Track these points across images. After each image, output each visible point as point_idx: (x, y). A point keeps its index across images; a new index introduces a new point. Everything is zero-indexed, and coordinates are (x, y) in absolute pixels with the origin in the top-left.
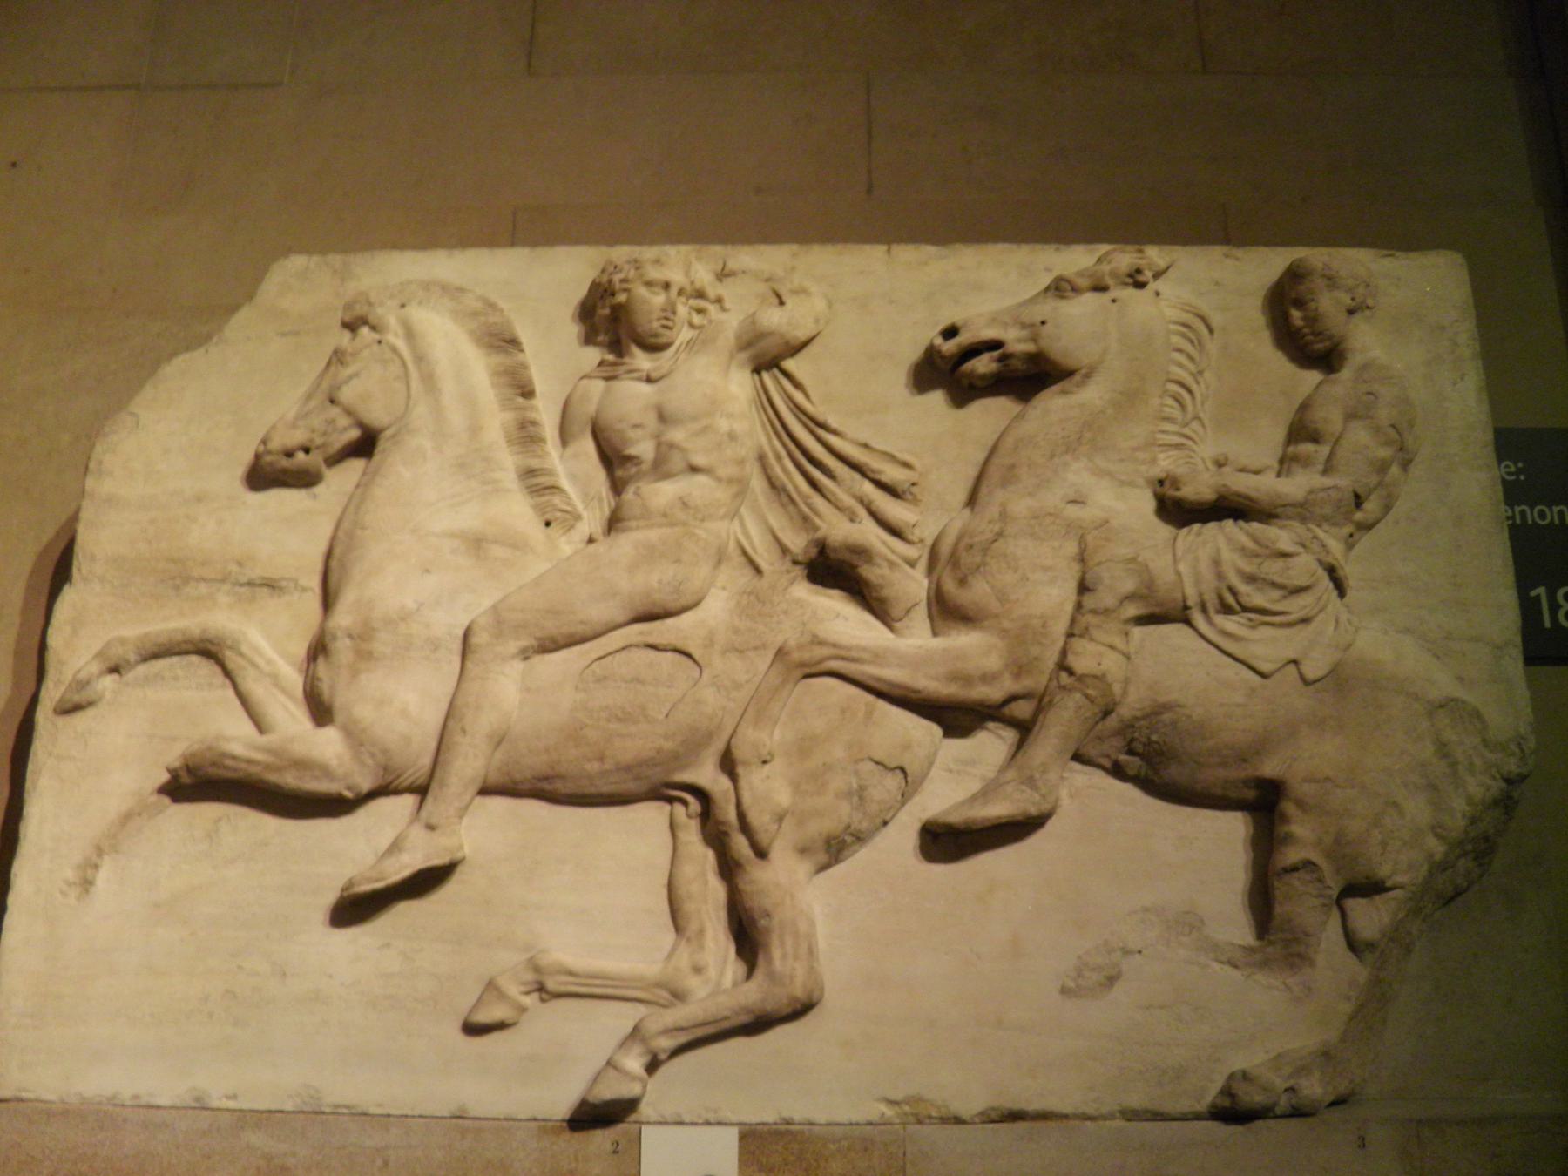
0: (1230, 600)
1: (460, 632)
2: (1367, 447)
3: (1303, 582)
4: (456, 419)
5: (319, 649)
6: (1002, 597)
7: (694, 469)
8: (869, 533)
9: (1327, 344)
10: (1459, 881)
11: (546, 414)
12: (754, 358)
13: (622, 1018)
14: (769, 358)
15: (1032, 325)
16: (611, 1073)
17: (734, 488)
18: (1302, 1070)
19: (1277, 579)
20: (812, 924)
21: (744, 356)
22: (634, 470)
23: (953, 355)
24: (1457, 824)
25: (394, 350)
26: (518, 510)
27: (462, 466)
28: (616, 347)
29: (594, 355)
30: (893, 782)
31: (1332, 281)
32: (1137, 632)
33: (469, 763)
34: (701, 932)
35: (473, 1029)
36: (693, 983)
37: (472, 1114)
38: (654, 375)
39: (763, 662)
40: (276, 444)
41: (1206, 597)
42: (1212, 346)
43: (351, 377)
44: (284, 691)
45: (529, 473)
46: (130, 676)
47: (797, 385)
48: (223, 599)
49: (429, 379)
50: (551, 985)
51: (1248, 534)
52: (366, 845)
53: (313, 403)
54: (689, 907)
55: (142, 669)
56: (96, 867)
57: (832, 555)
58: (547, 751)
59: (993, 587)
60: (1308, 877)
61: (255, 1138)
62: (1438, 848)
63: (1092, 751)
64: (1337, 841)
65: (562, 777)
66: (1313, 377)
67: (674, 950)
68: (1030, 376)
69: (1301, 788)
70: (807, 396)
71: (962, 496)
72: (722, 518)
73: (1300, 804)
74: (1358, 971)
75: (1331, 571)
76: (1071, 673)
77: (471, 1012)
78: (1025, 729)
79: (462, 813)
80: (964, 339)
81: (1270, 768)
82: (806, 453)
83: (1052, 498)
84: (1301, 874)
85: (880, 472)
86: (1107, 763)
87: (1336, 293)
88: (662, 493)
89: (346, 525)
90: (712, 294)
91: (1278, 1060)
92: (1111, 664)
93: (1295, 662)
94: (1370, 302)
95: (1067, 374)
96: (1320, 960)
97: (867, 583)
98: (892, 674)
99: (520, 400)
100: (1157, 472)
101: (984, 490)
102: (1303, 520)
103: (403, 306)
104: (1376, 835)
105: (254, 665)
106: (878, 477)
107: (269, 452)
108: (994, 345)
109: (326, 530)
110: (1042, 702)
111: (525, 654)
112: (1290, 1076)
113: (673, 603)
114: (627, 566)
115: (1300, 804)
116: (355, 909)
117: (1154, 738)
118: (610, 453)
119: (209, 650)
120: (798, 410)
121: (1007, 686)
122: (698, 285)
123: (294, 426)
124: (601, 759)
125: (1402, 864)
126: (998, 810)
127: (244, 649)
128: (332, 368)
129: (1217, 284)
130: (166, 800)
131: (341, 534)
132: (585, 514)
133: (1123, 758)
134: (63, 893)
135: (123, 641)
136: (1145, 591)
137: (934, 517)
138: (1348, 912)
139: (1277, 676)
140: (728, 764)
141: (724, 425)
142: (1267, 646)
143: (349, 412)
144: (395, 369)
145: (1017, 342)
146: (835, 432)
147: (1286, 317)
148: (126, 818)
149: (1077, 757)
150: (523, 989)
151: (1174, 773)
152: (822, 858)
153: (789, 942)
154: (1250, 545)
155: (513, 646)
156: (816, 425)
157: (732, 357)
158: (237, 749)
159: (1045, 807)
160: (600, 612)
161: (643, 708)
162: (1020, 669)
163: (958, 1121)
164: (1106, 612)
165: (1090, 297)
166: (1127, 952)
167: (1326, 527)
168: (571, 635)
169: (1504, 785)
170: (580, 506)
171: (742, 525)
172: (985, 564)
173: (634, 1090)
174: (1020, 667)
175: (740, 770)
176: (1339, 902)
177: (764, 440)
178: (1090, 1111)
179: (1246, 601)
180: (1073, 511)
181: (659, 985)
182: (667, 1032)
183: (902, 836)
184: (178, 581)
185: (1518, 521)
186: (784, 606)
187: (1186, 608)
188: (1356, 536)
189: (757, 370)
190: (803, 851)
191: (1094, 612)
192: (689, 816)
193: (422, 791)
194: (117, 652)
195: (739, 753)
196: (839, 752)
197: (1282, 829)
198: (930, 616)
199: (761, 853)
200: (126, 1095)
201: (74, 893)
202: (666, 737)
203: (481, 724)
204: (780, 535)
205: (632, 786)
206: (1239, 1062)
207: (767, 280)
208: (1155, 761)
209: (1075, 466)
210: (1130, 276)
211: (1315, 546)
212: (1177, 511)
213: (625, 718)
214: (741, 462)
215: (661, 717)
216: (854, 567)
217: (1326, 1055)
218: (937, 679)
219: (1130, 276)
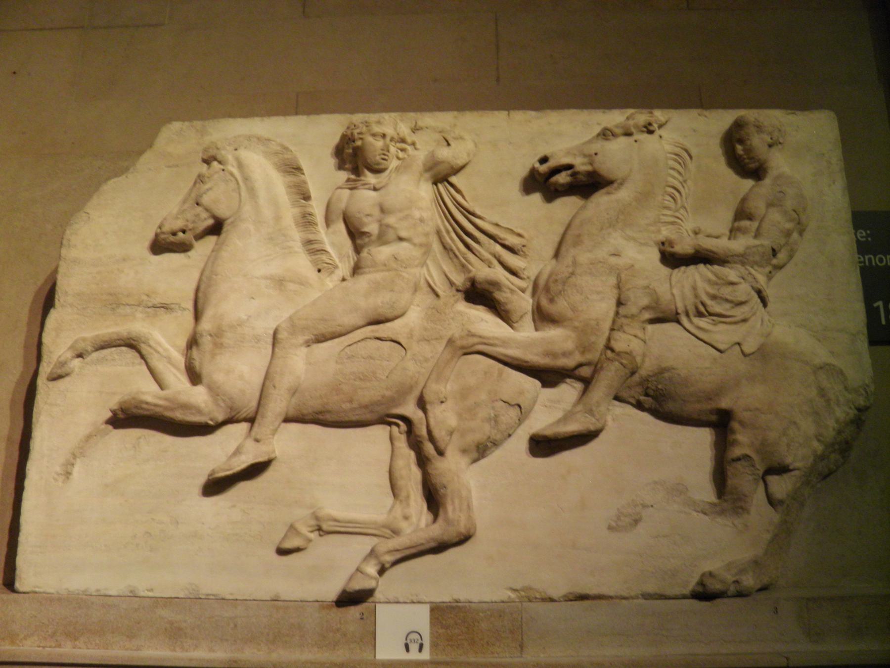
0: (702, 309)
1: (272, 332)
2: (779, 223)
3: (743, 299)
4: (267, 212)
5: (193, 342)
6: (574, 309)
7: (401, 239)
8: (500, 274)
9: (757, 164)
10: (832, 466)
11: (317, 209)
13: (364, 545)
14: (442, 176)
15: (590, 156)
16: (359, 574)
17: (423, 250)
18: (742, 571)
19: (729, 297)
20: (469, 491)
21: (427, 175)
22: (367, 240)
23: (545, 173)
24: (830, 434)
25: (232, 174)
26: (302, 264)
27: (271, 239)
28: (356, 171)
29: (343, 176)
30: (514, 413)
31: (759, 128)
32: (650, 328)
33: (278, 405)
34: (408, 497)
35: (282, 552)
36: (404, 525)
37: (282, 598)
38: (377, 186)
39: (440, 347)
40: (167, 228)
42: (691, 166)
43: (208, 190)
45: (309, 242)
46: (88, 359)
47: (458, 191)
48: (139, 315)
49: (252, 191)
50: (325, 527)
51: (712, 272)
52: (222, 451)
53: (186, 206)
54: (401, 483)
55: (95, 355)
56: (73, 465)
57: (479, 286)
61: (165, 613)
62: (819, 448)
63: (624, 394)
65: (329, 412)
66: (749, 183)
67: (393, 507)
68: (589, 184)
71: (551, 252)
72: (417, 266)
73: (741, 423)
74: (775, 517)
75: (759, 292)
76: (613, 350)
77: (281, 543)
78: (587, 382)
79: (274, 432)
80: (552, 163)
82: (463, 228)
83: (601, 253)
84: (743, 463)
85: (505, 239)
86: (634, 402)
88: (383, 253)
89: (207, 273)
90: (409, 140)
91: (728, 566)
92: (635, 346)
93: (739, 344)
94: (781, 141)
96: (753, 510)
97: (498, 302)
100: (661, 238)
101: (563, 249)
102: (743, 264)
103: (236, 150)
104: (784, 440)
107: (163, 233)
108: (569, 167)
109: (196, 275)
110: (597, 367)
111: (308, 344)
113: (389, 314)
114: (364, 294)
115: (741, 423)
116: (215, 486)
117: (660, 387)
118: (353, 230)
119: (132, 344)
120: (459, 205)
121: (577, 358)
122: (401, 135)
123: (177, 218)
124: (351, 401)
125: (799, 455)
126: (572, 427)
127: (152, 343)
128: (197, 185)
129: (694, 131)
130: (110, 427)
131: (204, 278)
132: (340, 265)
133: (642, 398)
135: (84, 340)
136: (654, 305)
137: (537, 264)
138: (768, 483)
140: (422, 404)
141: (417, 214)
142: (723, 334)
143: (207, 210)
144: (233, 185)
145: (581, 165)
147: (733, 149)
148: (89, 437)
149: (617, 398)
150: (310, 529)
151: (671, 406)
152: (475, 455)
153: (457, 501)
154: (713, 278)
155: (301, 339)
156: (469, 213)
157: (421, 175)
158: (149, 399)
159: (599, 425)
160: (349, 320)
161: (374, 373)
162: (584, 349)
163: (552, 600)
164: (632, 317)
165: (623, 140)
166: (645, 506)
167: (756, 268)
168: (334, 333)
169: (856, 412)
170: (337, 260)
171: (428, 270)
172: (564, 290)
175: (428, 407)
177: (439, 222)
178: (625, 594)
179: (711, 310)
180: (613, 260)
182: (390, 552)
183: (519, 443)
184: (114, 306)
185: (867, 264)
186: (452, 315)
187: (677, 313)
188: (773, 273)
189: (435, 183)
190: (464, 451)
191: (626, 317)
192: (400, 433)
193: (251, 420)
194: (81, 346)
195: (428, 397)
196: (483, 396)
197: (731, 437)
198: (534, 320)
199: (441, 453)
200: (92, 590)
202: (387, 389)
203: (284, 383)
204: (449, 275)
205: (369, 417)
206: (707, 567)
207: (440, 132)
208: (659, 399)
211: (750, 279)
212: (672, 259)
213: (363, 378)
214: (427, 235)
215: (384, 378)
216: (491, 293)
217: (756, 563)
218: (537, 355)
219: (645, 127)
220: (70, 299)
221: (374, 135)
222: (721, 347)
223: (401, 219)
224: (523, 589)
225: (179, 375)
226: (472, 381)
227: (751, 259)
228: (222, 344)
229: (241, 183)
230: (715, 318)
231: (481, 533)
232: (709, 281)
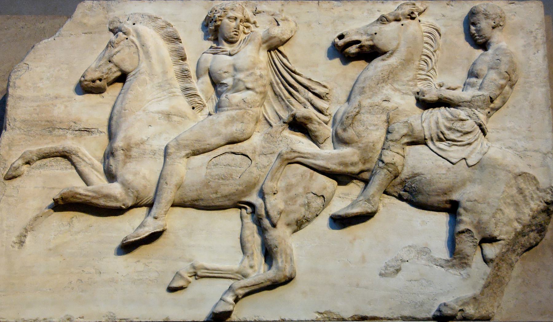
0: (442, 136)
1: (164, 148)
2: (495, 80)
3: (469, 130)
4: (158, 69)
5: (110, 154)
6: (359, 136)
7: (248, 89)
8: (311, 112)
9: (484, 40)
10: (532, 241)
11: (192, 68)
12: (268, 46)
14: (274, 46)
15: (372, 35)
16: (222, 302)
17: (262, 96)
18: (466, 303)
20: (292, 250)
21: (264, 46)
22: (225, 88)
23: (342, 46)
24: (526, 218)
25: (133, 42)
26: (183, 104)
27: (161, 86)
28: (216, 40)
29: (210, 44)
30: (320, 201)
31: (487, 16)
32: (408, 148)
33: (169, 194)
34: (253, 254)
35: (172, 290)
36: (250, 271)
38: (232, 53)
39: (274, 158)
40: (89, 77)
41: (433, 135)
42: (440, 41)
43: (117, 52)
44: (96, 170)
45: (187, 89)
46: (34, 165)
47: (284, 56)
50: (199, 273)
53: (102, 62)
54: (248, 245)
55: (38, 162)
56: (25, 236)
57: (298, 120)
58: (197, 190)
59: (355, 132)
60: (468, 235)
62: (519, 227)
63: (390, 190)
64: (479, 223)
65: (202, 200)
66: (480, 51)
67: (243, 260)
68: (370, 53)
69: (465, 203)
70: (288, 61)
71: (345, 98)
72: (258, 107)
73: (465, 209)
75: (480, 126)
76: (383, 162)
77: (170, 284)
78: (366, 182)
79: (166, 213)
80: (346, 40)
81: (455, 197)
82: (288, 82)
83: (377, 99)
85: (315, 89)
86: (397, 195)
87: (488, 21)
88: (237, 97)
89: (118, 108)
90: (252, 20)
91: (457, 301)
92: (398, 159)
93: (465, 159)
94: (501, 24)
95: (385, 53)
96: (473, 265)
97: (311, 130)
98: (320, 163)
99: (181, 61)
100: (417, 89)
101: (353, 96)
102: (470, 107)
103: (134, 24)
105: (84, 160)
106: (314, 91)
107: (86, 81)
108: (358, 42)
109: (109, 110)
110: (372, 172)
111: (188, 156)
112: (461, 305)
113: (240, 137)
114: (223, 125)
115: (465, 209)
116: (127, 248)
117: (413, 185)
118: (215, 81)
119: (65, 155)
120: (285, 66)
122: (247, 17)
123: (96, 71)
124: (216, 193)
125: (504, 231)
126: (356, 210)
127: (80, 155)
128: (109, 48)
129: (443, 16)
130: (52, 211)
131: (115, 111)
132: (207, 104)
133: (402, 193)
134: (13, 247)
135: (31, 152)
137: (335, 107)
138: (483, 248)
139: (458, 164)
140: (262, 194)
141: (258, 72)
142: (455, 153)
143: (116, 66)
144: (133, 49)
145: (365, 40)
146: (298, 74)
147: (469, 28)
148: (36, 218)
149: (385, 192)
150: (190, 275)
151: (420, 198)
152: (295, 227)
153: (284, 256)
154: (450, 116)
155: (184, 153)
156: (292, 72)
157: (260, 46)
158: (82, 191)
159: (374, 209)
160: (214, 141)
161: (231, 175)
162: (365, 161)
164: (396, 141)
165: (394, 24)
166: (403, 261)
167: (479, 110)
168: (205, 149)
169: (545, 205)
170: (205, 102)
171: (265, 108)
172: (353, 123)
173: (228, 308)
174: (365, 160)
175: (266, 196)
176: (480, 244)
178: (390, 317)
179: (447, 137)
180: (385, 104)
181: (237, 272)
182: (241, 288)
183: (323, 220)
184: (51, 129)
186: (280, 138)
187: (425, 139)
188: (491, 113)
189: (269, 51)
190: (288, 225)
191: (392, 141)
192: (248, 214)
193: (150, 206)
194: (29, 157)
195: (266, 190)
196: (301, 190)
197: (459, 218)
199: (274, 226)
201: (17, 246)
202: (239, 185)
203: (173, 181)
204: (278, 112)
205: (227, 203)
206: (443, 300)
207: (272, 15)
208: (414, 195)
209: (386, 87)
210: (409, 15)
211: (474, 117)
212: (424, 104)
214: (264, 86)
215: (238, 178)
216: (306, 124)
217: (475, 298)
219: (409, 15)
220: (18, 124)
221: (229, 18)
222: (453, 161)
223: (248, 76)
224: (326, 313)
225: (99, 175)
226: (294, 181)
227: (476, 104)
228: (130, 156)
229: (140, 48)
230: (450, 142)
231: (298, 277)
232: (447, 119)
